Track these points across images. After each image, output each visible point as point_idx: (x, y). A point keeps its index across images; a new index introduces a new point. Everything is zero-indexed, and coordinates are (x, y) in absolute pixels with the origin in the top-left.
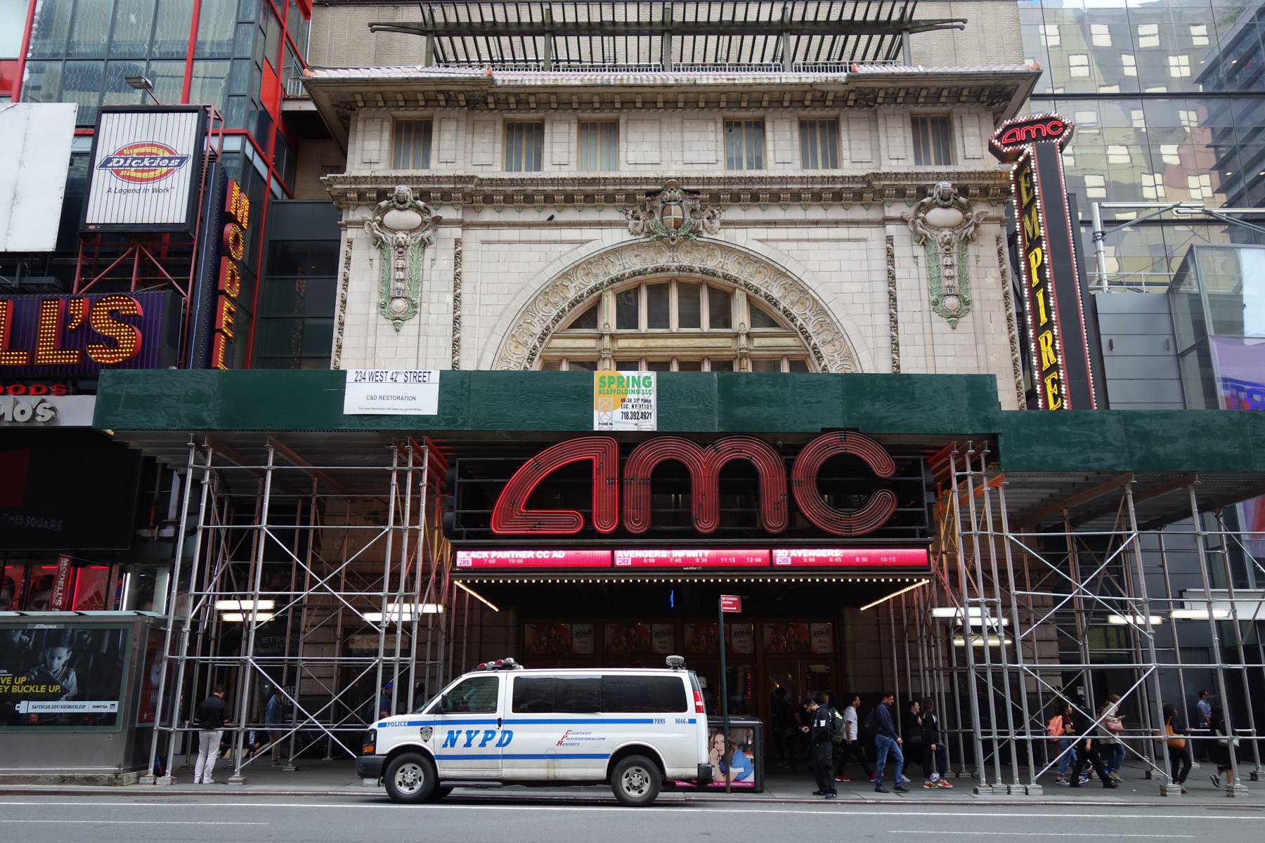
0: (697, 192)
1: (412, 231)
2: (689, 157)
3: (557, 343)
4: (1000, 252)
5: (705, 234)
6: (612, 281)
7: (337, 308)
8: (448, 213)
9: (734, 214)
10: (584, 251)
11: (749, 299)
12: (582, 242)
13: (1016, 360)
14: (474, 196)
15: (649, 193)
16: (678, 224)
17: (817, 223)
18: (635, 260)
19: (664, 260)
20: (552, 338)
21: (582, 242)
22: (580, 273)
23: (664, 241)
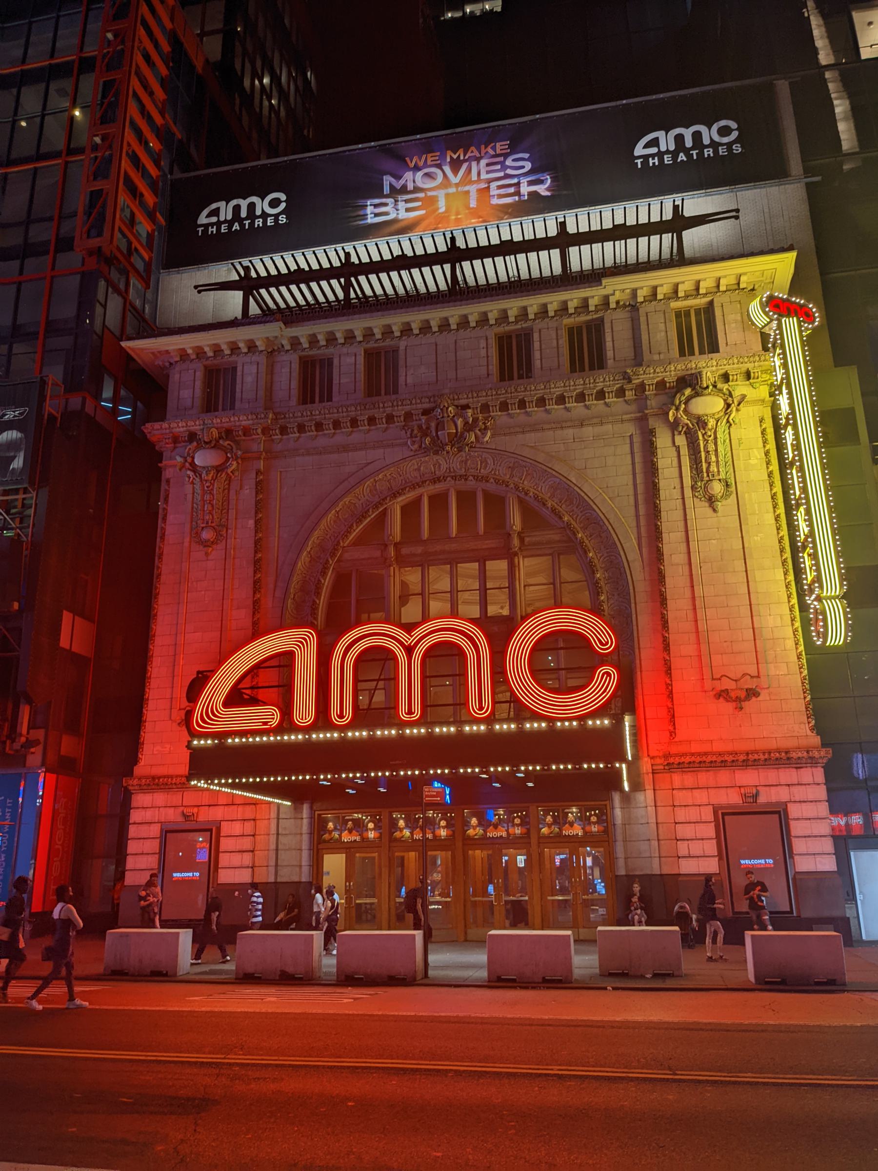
4: (763, 432)
7: (158, 540)
11: (521, 501)
13: (782, 538)
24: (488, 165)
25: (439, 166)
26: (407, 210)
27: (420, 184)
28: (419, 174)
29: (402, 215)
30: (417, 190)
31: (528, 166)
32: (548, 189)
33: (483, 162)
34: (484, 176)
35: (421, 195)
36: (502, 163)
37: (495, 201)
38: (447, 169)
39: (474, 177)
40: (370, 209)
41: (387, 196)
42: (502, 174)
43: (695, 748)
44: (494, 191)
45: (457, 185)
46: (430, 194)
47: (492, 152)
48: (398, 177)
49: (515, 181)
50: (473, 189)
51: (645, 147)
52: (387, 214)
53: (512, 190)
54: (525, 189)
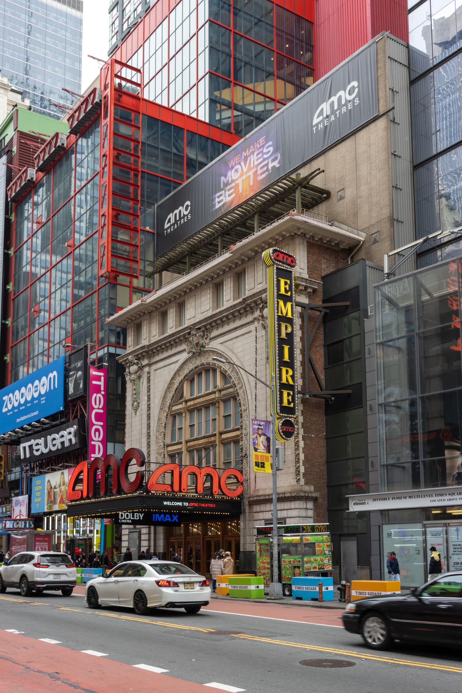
0: (199, 329)
1: (136, 373)
2: (203, 309)
3: (174, 408)
5: (207, 347)
6: (185, 377)
8: (145, 362)
9: (215, 333)
10: (176, 367)
11: (221, 372)
12: (177, 362)
14: (151, 352)
15: (189, 333)
16: (197, 344)
17: (236, 329)
18: (191, 364)
19: (198, 362)
20: (173, 406)
21: (177, 362)
22: (177, 375)
23: (194, 355)
24: (257, 155)
25: (240, 163)
26: (229, 195)
27: (234, 178)
28: (233, 171)
29: (228, 199)
30: (233, 181)
31: (271, 149)
32: (279, 163)
33: (255, 154)
34: (256, 163)
35: (233, 184)
36: (262, 152)
37: (260, 178)
38: (242, 163)
39: (252, 166)
40: (217, 200)
41: (222, 190)
42: (261, 159)
43: (261, 493)
44: (259, 172)
45: (246, 173)
46: (237, 182)
47: (259, 146)
48: (225, 176)
49: (266, 162)
50: (251, 173)
51: (318, 117)
52: (222, 200)
53: (265, 168)
54: (270, 166)
